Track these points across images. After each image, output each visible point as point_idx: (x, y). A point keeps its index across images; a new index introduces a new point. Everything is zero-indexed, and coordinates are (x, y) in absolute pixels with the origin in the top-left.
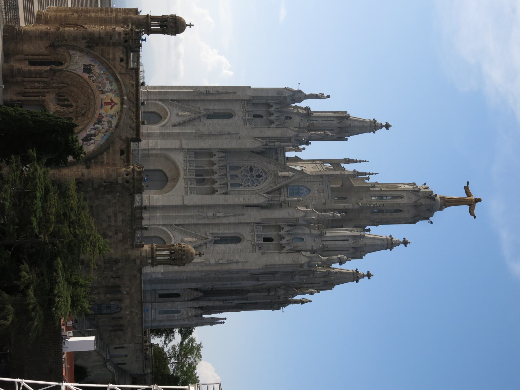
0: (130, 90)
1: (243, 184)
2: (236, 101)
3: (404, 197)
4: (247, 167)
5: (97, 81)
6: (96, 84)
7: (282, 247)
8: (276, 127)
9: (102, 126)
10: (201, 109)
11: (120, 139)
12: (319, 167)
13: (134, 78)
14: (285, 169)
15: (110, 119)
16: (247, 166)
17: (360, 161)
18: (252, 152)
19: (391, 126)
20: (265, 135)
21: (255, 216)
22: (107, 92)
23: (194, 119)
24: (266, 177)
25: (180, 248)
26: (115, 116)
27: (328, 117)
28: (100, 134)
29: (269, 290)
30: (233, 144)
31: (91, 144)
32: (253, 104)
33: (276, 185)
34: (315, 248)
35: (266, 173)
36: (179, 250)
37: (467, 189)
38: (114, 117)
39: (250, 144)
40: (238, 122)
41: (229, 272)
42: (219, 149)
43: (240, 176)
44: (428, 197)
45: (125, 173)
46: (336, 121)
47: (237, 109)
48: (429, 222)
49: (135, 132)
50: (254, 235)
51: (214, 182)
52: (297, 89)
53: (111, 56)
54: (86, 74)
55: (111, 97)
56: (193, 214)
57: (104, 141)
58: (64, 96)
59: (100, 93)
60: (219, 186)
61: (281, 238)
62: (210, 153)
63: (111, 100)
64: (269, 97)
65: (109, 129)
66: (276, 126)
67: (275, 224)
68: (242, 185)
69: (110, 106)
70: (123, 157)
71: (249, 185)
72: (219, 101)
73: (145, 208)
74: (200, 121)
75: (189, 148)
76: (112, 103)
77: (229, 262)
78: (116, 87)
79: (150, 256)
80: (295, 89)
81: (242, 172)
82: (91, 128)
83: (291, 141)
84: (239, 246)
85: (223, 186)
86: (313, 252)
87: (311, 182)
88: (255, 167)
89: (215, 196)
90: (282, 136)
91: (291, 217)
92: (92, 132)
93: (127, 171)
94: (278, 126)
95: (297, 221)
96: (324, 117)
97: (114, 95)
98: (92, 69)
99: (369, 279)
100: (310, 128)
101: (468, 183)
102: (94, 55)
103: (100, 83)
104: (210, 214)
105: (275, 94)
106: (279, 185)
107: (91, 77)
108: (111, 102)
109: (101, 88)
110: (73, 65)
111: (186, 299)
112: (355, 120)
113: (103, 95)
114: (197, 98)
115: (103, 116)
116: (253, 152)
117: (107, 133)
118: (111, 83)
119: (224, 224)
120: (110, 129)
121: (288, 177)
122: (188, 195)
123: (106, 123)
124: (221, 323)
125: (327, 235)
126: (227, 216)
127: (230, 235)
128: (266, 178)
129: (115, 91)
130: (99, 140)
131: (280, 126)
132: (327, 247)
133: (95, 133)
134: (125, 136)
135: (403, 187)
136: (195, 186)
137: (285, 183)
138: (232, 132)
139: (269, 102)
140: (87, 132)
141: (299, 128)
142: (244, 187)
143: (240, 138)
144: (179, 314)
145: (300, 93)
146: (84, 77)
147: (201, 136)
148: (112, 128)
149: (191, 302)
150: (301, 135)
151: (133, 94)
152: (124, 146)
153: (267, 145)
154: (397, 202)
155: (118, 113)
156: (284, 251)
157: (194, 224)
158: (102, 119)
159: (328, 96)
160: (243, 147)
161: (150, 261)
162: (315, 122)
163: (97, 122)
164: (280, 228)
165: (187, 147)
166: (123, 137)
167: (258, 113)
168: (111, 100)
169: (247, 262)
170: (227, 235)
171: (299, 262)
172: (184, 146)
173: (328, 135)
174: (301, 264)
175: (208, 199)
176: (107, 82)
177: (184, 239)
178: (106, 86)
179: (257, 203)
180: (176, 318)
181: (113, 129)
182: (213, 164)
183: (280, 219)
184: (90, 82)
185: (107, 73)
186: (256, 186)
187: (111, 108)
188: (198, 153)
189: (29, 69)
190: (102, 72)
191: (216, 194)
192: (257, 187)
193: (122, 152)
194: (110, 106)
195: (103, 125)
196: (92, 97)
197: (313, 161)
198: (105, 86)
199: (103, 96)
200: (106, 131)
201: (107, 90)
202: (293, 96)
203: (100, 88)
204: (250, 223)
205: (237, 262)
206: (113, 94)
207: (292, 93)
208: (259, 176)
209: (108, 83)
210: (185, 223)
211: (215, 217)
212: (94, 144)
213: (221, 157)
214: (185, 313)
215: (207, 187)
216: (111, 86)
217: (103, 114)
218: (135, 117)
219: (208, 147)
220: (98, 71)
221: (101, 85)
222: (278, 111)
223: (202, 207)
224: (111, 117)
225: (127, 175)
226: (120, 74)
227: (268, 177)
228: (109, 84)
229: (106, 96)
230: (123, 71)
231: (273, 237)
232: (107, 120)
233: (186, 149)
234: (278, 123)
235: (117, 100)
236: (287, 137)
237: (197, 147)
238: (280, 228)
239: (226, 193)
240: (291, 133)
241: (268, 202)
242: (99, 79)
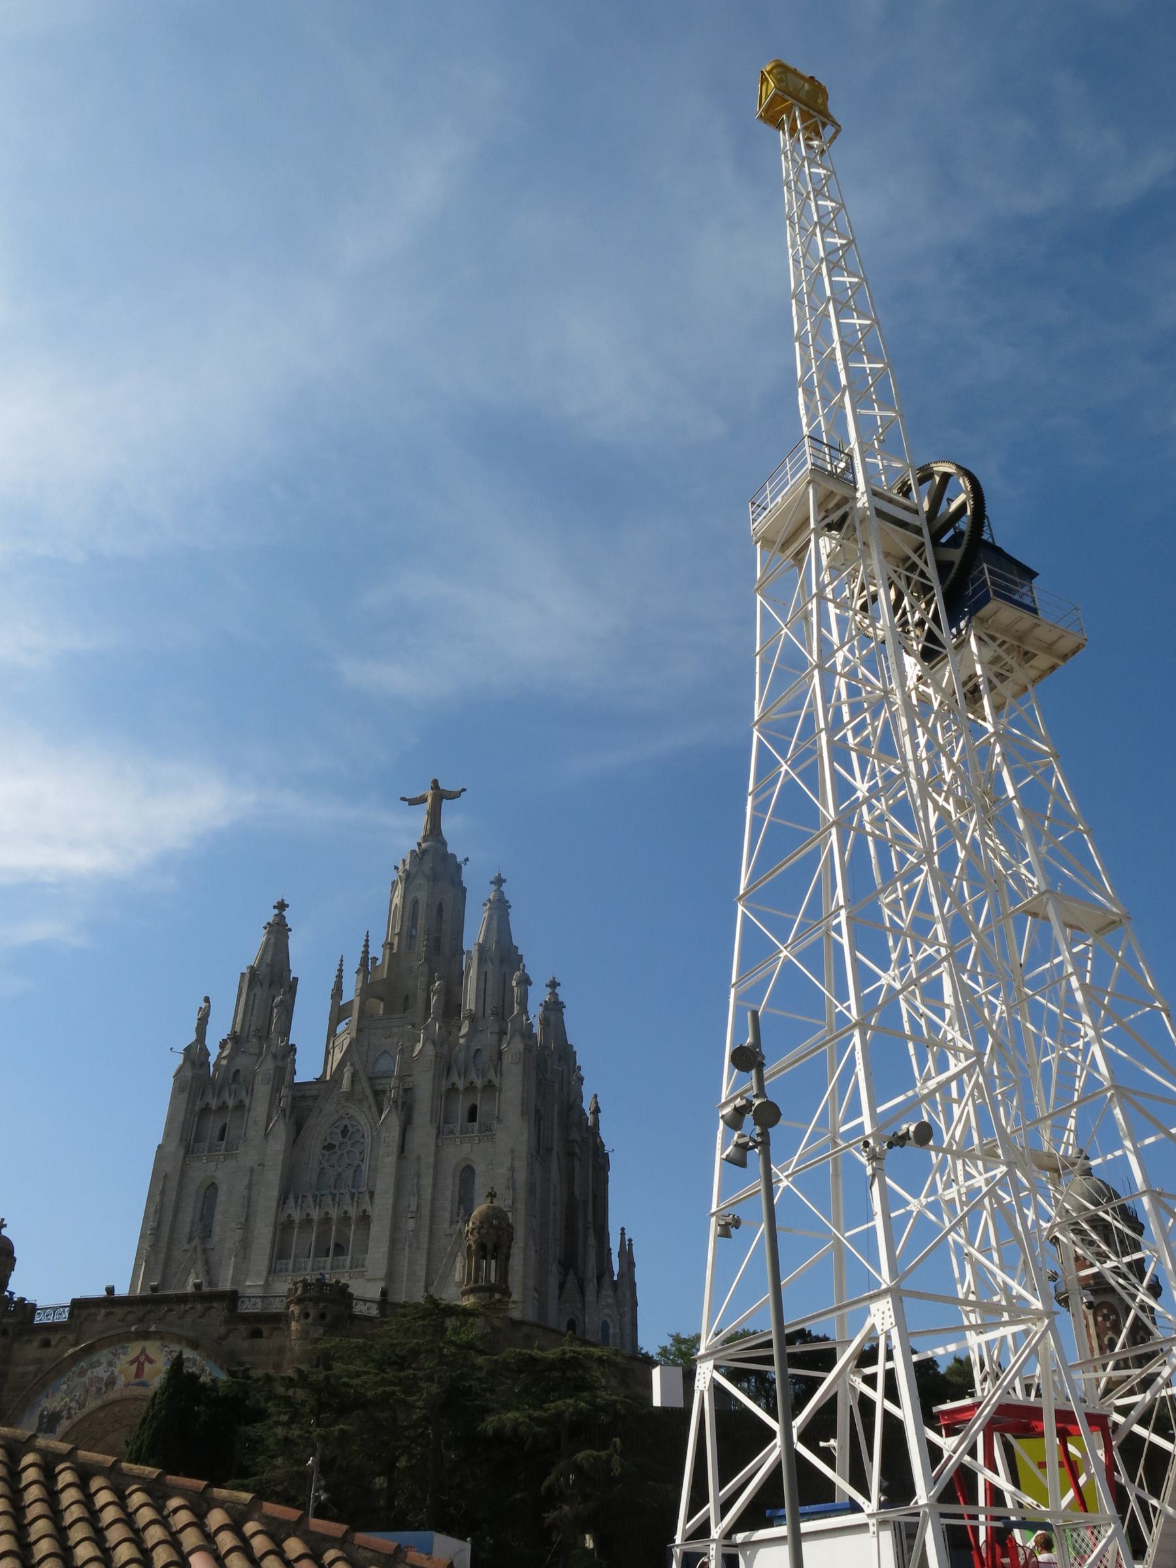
0: (119, 1321)
1: (357, 1162)
2: (183, 1173)
4: (323, 1155)
7: (490, 1087)
8: (252, 1095)
10: (186, 1247)
11: (224, 1338)
12: (341, 1040)
13: (93, 1310)
14: (336, 1081)
17: (340, 970)
18: (294, 1143)
19: (283, 900)
20: (265, 1115)
21: (423, 1136)
22: (113, 1373)
23: (207, 1262)
25: (475, 1233)
27: (246, 1005)
29: (571, 1154)
30: (272, 1179)
32: (195, 1141)
33: (367, 1097)
34: (496, 1029)
35: (341, 1118)
36: (478, 1233)
37: (413, 802)
39: (277, 1146)
41: (531, 1189)
42: (278, 1206)
43: (339, 1170)
44: (421, 859)
45: (302, 1321)
46: (258, 990)
47: (200, 1172)
48: (466, 864)
49: (215, 1304)
50: (461, 1138)
51: (345, 1219)
52: (182, 1056)
53: (31, 1368)
56: (406, 1261)
59: (113, 1388)
60: (355, 1208)
61: (471, 1088)
62: (284, 1228)
63: (132, 1363)
64: (187, 1108)
66: (249, 1096)
67: (443, 1098)
68: (359, 1166)
70: (265, 1329)
71: (361, 1150)
72: (177, 1211)
73: (384, 1293)
74: (212, 1249)
76: (140, 1362)
77: (510, 1185)
78: (105, 1352)
79: (487, 1294)
80: (179, 1060)
81: (333, 1166)
83: (283, 1068)
84: (479, 1169)
85: (356, 1199)
86: (502, 1032)
87: (368, 1050)
88: (326, 1139)
89: (374, 1212)
90: (271, 1084)
91: (433, 1068)
93: (299, 1317)
94: (250, 1092)
95: (441, 1058)
96: (245, 1011)
97: (122, 1356)
98: (50, 1412)
99: (559, 984)
100: (263, 1035)
101: (403, 799)
103: (87, 1391)
104: (411, 1224)
105: (185, 1095)
106: (368, 1092)
107: (69, 1413)
108: (136, 1364)
111: (579, 1305)
112: (261, 959)
114: (162, 1256)
117: (206, 1368)
118: (92, 1366)
119: (433, 1199)
120: (197, 1363)
121: (354, 1075)
122: (366, 1271)
124: (630, 1245)
125: (473, 1007)
126: (418, 1190)
127: (457, 1188)
128: (351, 1118)
129: (114, 1354)
131: (250, 1089)
132: (497, 1008)
134: (221, 1326)
135: (397, 900)
136: (349, 1257)
137: (365, 1084)
138: (246, 1182)
141: (260, 1054)
142: (362, 1161)
143: (262, 1165)
144: (611, 1325)
145: (189, 1051)
147: (245, 1245)
149: (588, 1294)
150: (273, 1050)
151: (129, 1312)
152: (243, 1329)
153: (284, 1111)
154: (425, 906)
155: (165, 1346)
156: (496, 1082)
157: (429, 1260)
159: (207, 1000)
160: (281, 1157)
161: (497, 1296)
162: (253, 1028)
164: (453, 1090)
165: (265, 1274)
166: (223, 1330)
167: (217, 1133)
168: (132, 1363)
169: (512, 1151)
170: (457, 1194)
171: (520, 1053)
173: (281, 1000)
174: (525, 1049)
175: (380, 1231)
176: (89, 1374)
177: (457, 1280)
179: (398, 1129)
180: (618, 1330)
181: (200, 1355)
182: (308, 1221)
183: (433, 1089)
185: (71, 1374)
187: (151, 1361)
188: (280, 1251)
190: (65, 1387)
192: (366, 1135)
193: (256, 1334)
194: (147, 1365)
197: (327, 1053)
199: (121, 1380)
201: (109, 1373)
202: (193, 1064)
203: (99, 1390)
204: (437, 1147)
205: (512, 1169)
206: (119, 1359)
207: (188, 1065)
208: (345, 1132)
209: (92, 1373)
210: (423, 1279)
211: (417, 1215)
213: (296, 1202)
214: (607, 1311)
215: (355, 1234)
216: (99, 1364)
218: (183, 1305)
219: (271, 1229)
220: (58, 1396)
221: (94, 1389)
222: (220, 1092)
223: (394, 1242)
225: (307, 1316)
226: (76, 1344)
227: (349, 1115)
230: (71, 1337)
231: (467, 1105)
233: (268, 1277)
234: (244, 1094)
235: (134, 1349)
236: (275, 1074)
237: (268, 1251)
238: (453, 1090)
239: (372, 1194)
240: (269, 1065)
241: (399, 1108)
242: (78, 1394)
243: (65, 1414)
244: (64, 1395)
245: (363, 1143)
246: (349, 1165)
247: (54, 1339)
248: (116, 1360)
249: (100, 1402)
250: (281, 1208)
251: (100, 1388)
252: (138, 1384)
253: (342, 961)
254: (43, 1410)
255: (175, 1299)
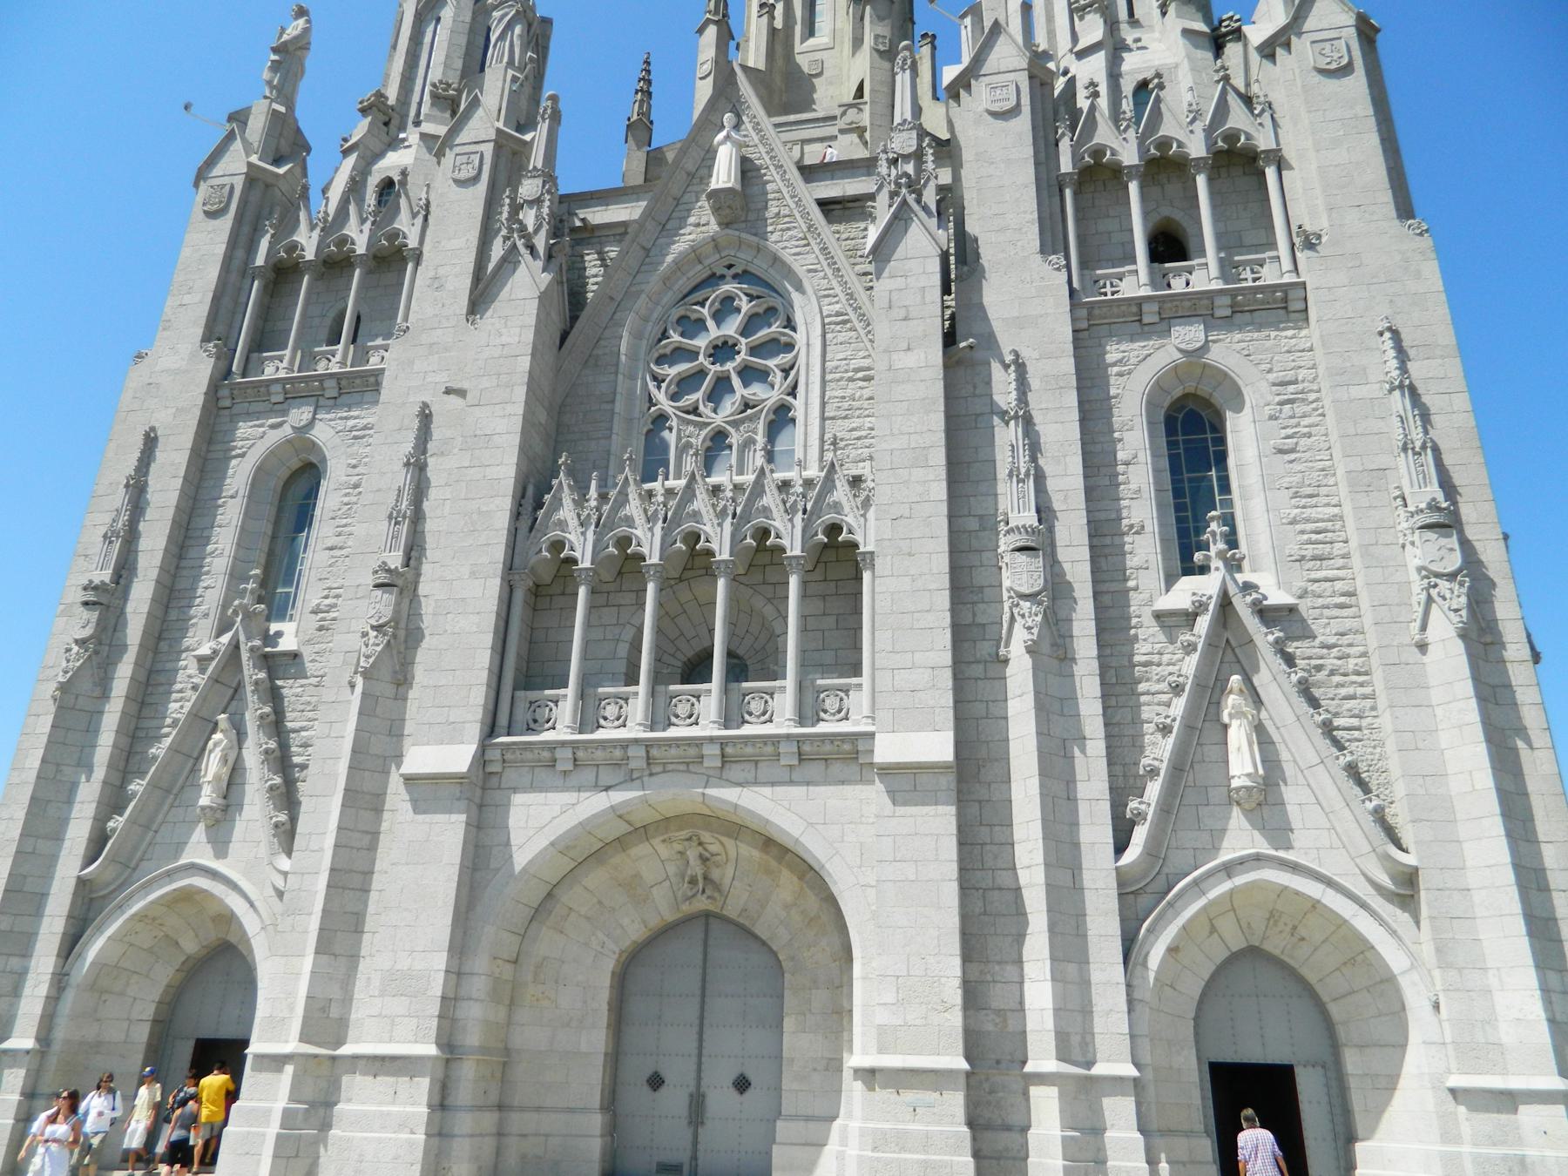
4: (658, 380)
16: (651, 385)
24: (735, 276)
40: (351, 423)
42: (517, 515)
66: (419, 220)
67: (1068, 193)
75: (479, 716)
89: (867, 533)
116: (564, 337)
138: (408, 447)
139: (260, 260)
142: (793, 392)
160: (525, 363)
165: (474, 731)
172: (458, 757)
186: (794, 329)
191: (858, 538)
211: (1041, 544)
219: (494, 585)
227: (738, 269)
245: (789, 347)
246: (747, 406)
250: (524, 524)
253: (647, 62)
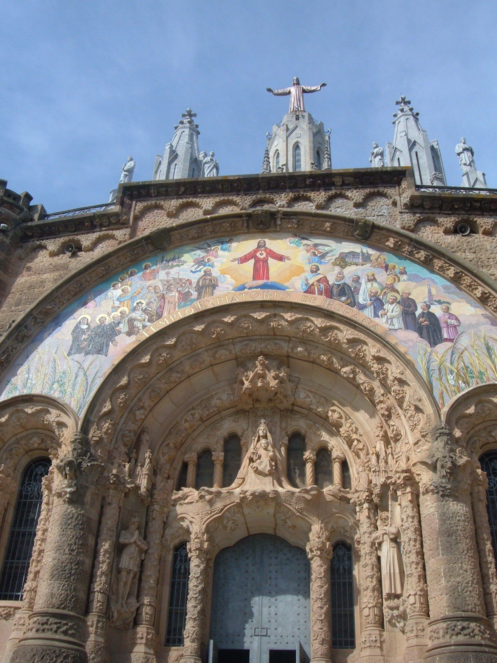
3: (297, 142)
5: (154, 306)
6: (167, 307)
9: (363, 281)
15: (331, 258)
26: (316, 245)
28: (400, 286)
31: (453, 315)
38: (320, 247)
49: (381, 189)
54: (115, 345)
55: (232, 261)
57: (424, 272)
58: (185, 465)
59: (213, 295)
63: (244, 260)
65: (377, 259)
69: (271, 261)
82: (376, 315)
92: (394, 314)
97: (220, 252)
98: (93, 326)
102: (35, 313)
103: (163, 297)
108: (252, 261)
109: (189, 291)
110: (64, 392)
113: (220, 284)
115: (318, 281)
117: (391, 264)
123: (350, 271)
130: (424, 289)
133: (399, 303)
140: (396, 330)
146: (129, 350)
148: (371, 251)
154: (308, 149)
158: (330, 283)
163: (343, 299)
168: (244, 260)
178: (180, 277)
184: (153, 328)
187: (280, 258)
189: (52, 576)
194: (271, 261)
195: (357, 280)
196: (229, 319)
198: (181, 280)
200: (386, 268)
201: (202, 273)
203: (185, 297)
209: (168, 274)
212: (450, 304)
217: (307, 280)
224: (323, 256)
228: (170, 270)
229: (228, 276)
232: (337, 269)
243: (123, 327)
244: (117, 303)
247: (86, 240)
248: (211, 258)
249: (190, 311)
251: (188, 294)
252: (264, 287)
254: (80, 323)
255: (308, 182)
